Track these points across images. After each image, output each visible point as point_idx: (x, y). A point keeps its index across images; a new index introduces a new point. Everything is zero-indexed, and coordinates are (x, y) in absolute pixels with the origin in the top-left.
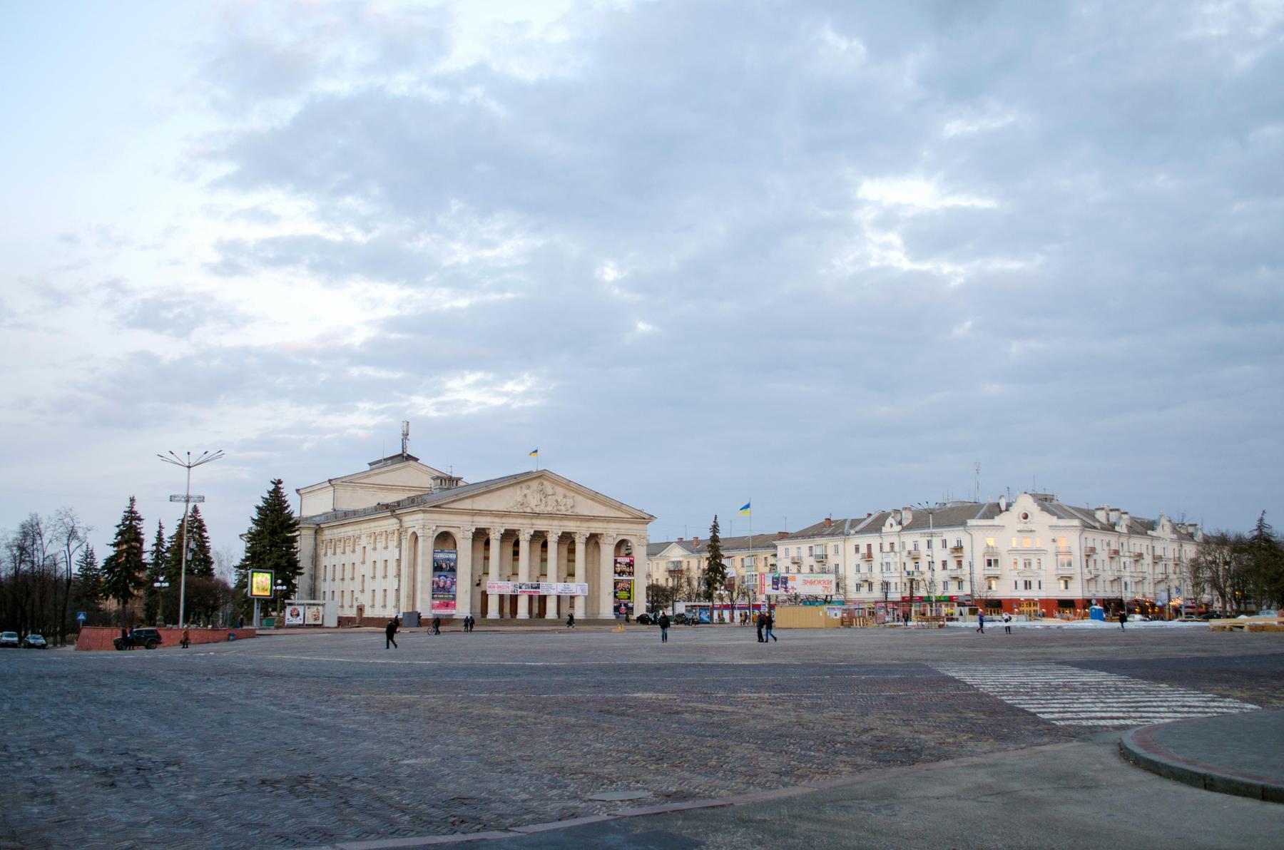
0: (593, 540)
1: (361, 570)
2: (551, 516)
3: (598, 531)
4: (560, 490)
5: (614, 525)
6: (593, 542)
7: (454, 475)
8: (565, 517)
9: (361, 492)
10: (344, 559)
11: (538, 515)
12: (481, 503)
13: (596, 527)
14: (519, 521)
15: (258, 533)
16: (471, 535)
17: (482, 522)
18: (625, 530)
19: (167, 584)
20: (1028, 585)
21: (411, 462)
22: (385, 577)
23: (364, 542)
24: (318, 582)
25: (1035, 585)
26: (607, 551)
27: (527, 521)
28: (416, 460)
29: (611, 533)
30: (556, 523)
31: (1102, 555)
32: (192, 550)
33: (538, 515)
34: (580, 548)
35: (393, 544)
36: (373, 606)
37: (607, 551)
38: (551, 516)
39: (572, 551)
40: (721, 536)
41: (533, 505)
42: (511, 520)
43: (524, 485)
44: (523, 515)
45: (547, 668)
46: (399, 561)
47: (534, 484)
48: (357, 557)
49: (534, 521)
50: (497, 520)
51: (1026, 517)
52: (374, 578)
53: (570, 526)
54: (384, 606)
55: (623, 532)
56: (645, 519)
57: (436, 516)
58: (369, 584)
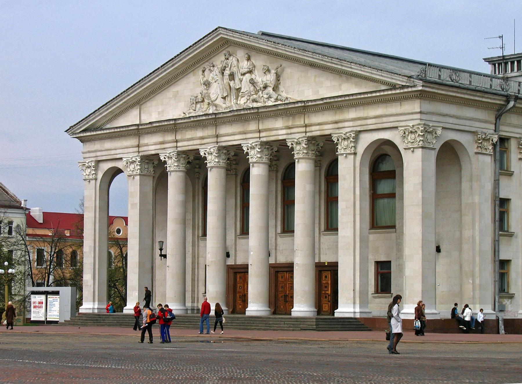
0: (325, 155)
2: (240, 117)
3: (327, 129)
4: (259, 62)
5: (352, 114)
8: (258, 114)
12: (154, 112)
13: (321, 124)
14: (199, 133)
17: (151, 144)
27: (210, 132)
29: (355, 134)
30: (253, 126)
33: (215, 120)
38: (240, 117)
41: (219, 101)
42: (189, 134)
43: (206, 65)
44: (196, 123)
47: (219, 60)
49: (224, 130)
50: (170, 137)
55: (371, 123)
57: (97, 146)
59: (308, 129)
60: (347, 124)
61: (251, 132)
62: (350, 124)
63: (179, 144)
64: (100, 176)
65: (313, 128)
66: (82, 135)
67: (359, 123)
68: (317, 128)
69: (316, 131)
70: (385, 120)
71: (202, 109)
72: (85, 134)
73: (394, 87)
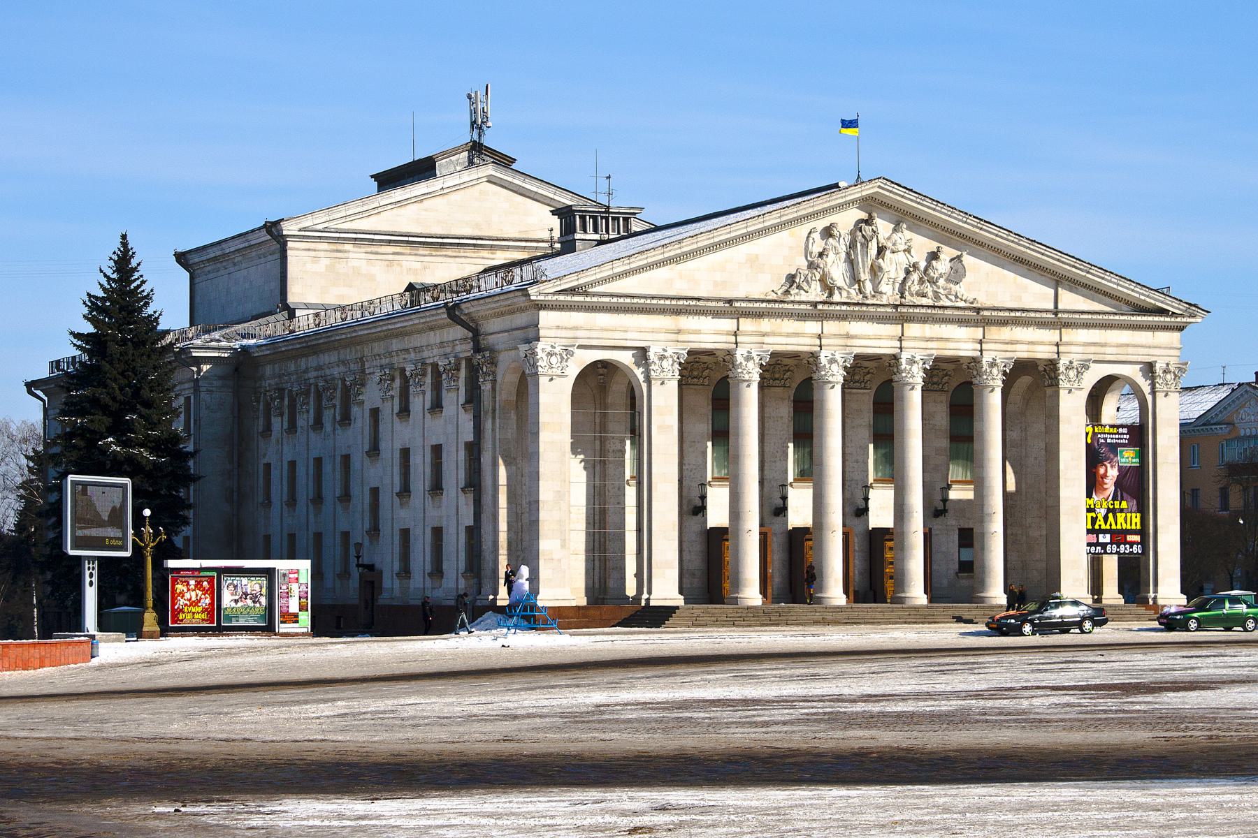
3: (1043, 352)
7: (616, 204)
9: (357, 256)
10: (317, 444)
11: (860, 312)
13: (1035, 343)
14: (813, 327)
17: (709, 333)
23: (372, 395)
35: (454, 398)
36: (405, 572)
38: (899, 315)
45: (948, 699)
48: (355, 437)
52: (405, 490)
53: (959, 341)
55: (1110, 352)
59: (1009, 347)
60: (1073, 349)
61: (915, 339)
62: (1080, 349)
63: (766, 340)
64: (574, 370)
65: (1018, 347)
66: (562, 298)
67: (1093, 349)
68: (1025, 347)
69: (1023, 353)
70: (1130, 350)
72: (569, 298)
73: (1162, 312)
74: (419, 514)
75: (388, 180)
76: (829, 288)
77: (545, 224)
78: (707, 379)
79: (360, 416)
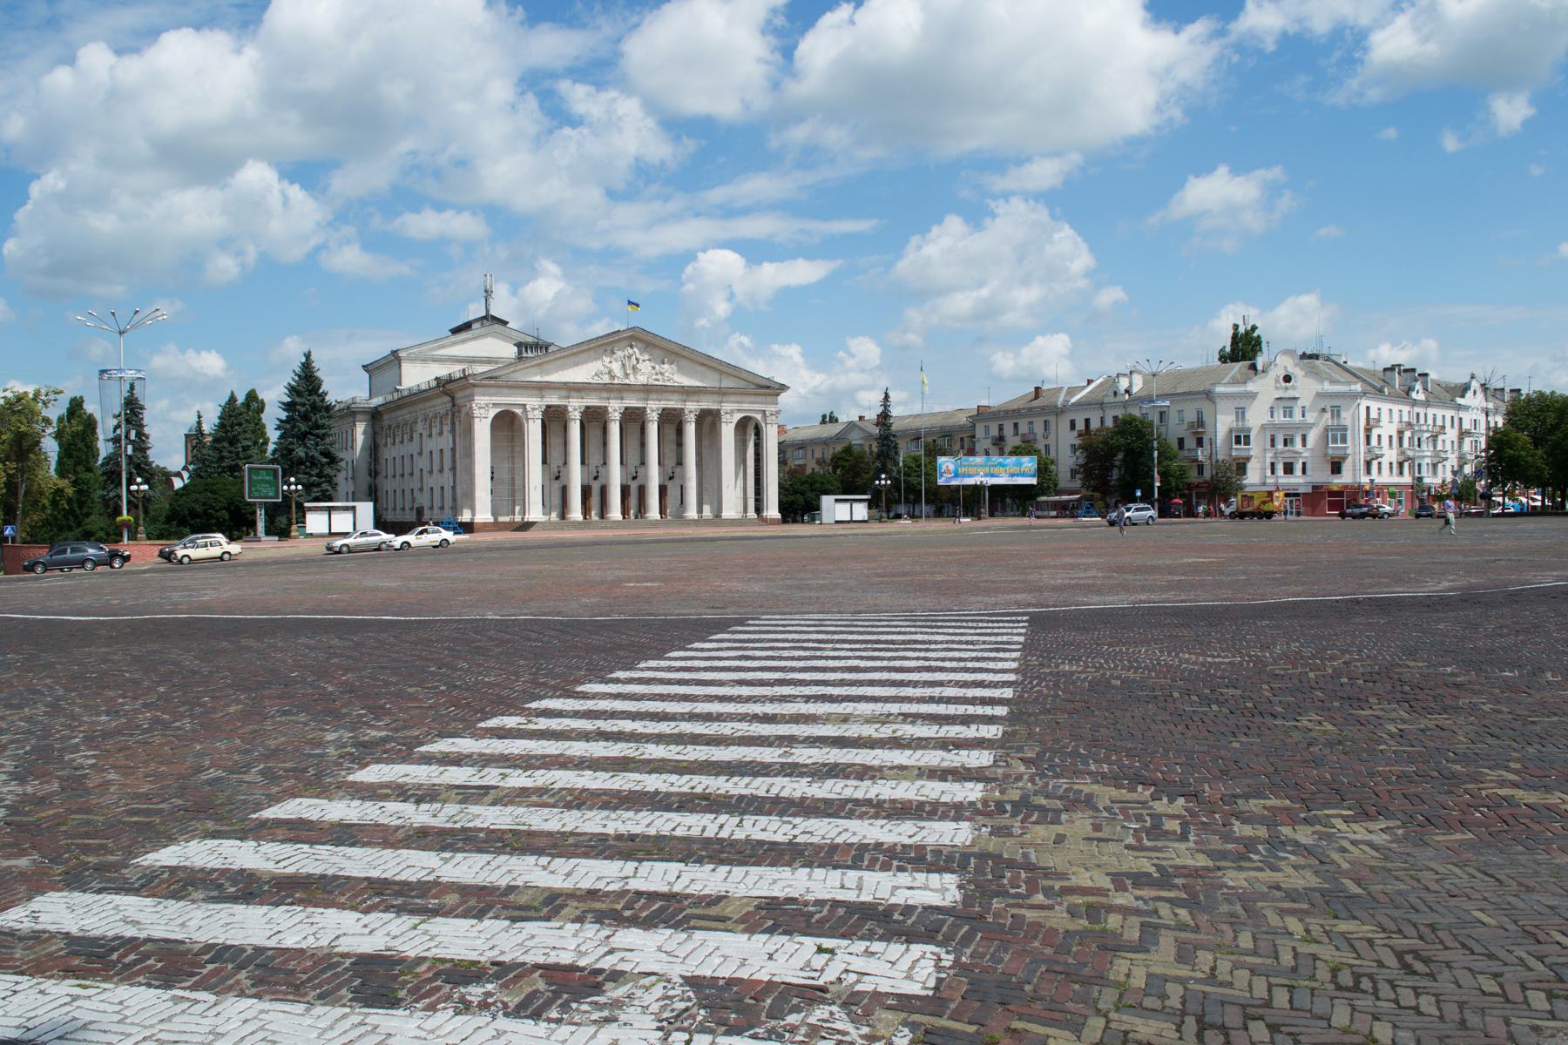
0: (709, 422)
1: (422, 463)
6: (709, 419)
15: (289, 420)
16: (538, 414)
18: (752, 408)
19: (146, 487)
20: (1289, 469)
21: (497, 327)
22: (441, 470)
23: (420, 428)
24: (380, 478)
25: (1298, 467)
26: (728, 433)
28: (505, 323)
31: (1387, 429)
32: (132, 442)
34: (690, 430)
36: (431, 508)
37: (728, 433)
39: (680, 432)
40: (895, 412)
46: (453, 450)
51: (1287, 379)
52: (431, 472)
54: (442, 508)
55: (746, 406)
56: (772, 390)
58: (430, 482)
71: (606, 379)
74: (432, 481)
75: (455, 331)
76: (613, 377)
77: (512, 351)
78: (554, 419)
79: (416, 436)
